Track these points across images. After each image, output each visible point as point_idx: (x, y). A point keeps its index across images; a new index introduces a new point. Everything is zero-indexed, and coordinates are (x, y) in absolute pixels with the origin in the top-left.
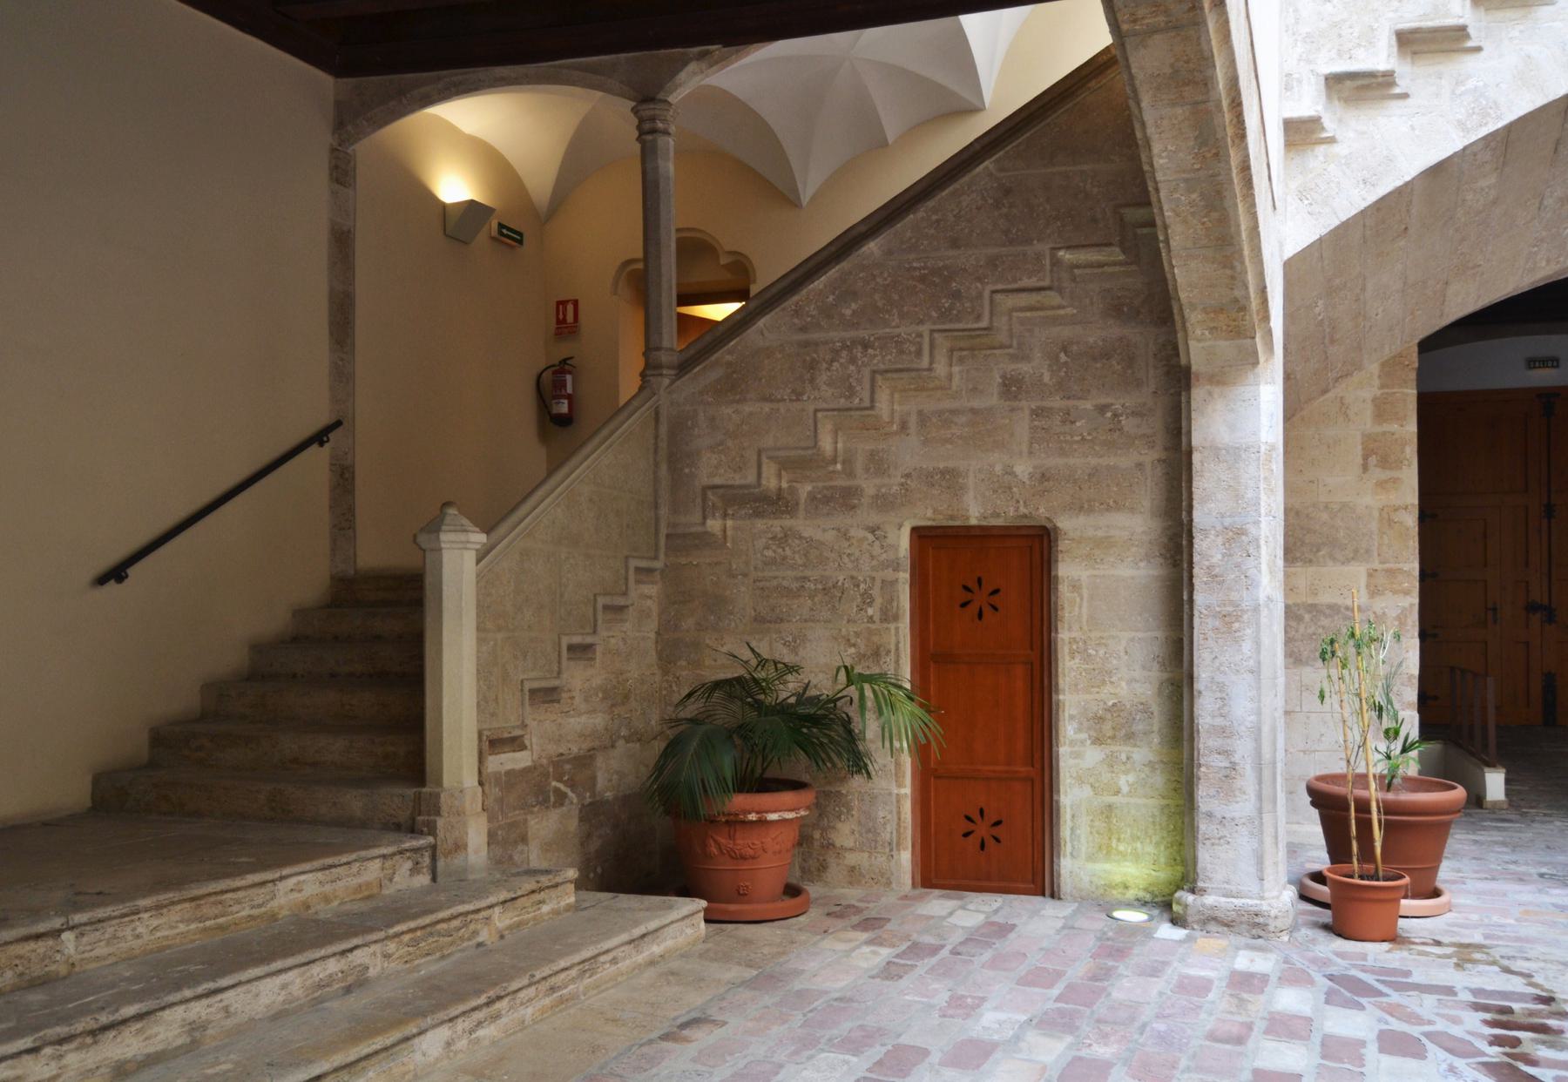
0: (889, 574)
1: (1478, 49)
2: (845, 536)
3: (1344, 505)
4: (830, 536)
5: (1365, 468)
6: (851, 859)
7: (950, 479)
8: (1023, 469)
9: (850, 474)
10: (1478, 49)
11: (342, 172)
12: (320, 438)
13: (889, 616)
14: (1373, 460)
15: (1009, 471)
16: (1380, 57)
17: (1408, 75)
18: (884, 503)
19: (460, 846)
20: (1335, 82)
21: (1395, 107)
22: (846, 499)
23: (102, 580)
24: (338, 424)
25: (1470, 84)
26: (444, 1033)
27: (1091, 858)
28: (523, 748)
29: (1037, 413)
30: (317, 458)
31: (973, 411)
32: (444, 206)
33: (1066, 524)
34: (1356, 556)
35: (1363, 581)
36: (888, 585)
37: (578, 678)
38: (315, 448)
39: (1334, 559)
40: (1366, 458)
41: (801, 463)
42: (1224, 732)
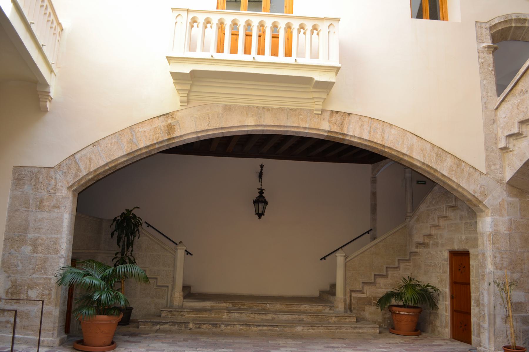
0: (444, 262)
4: (434, 253)
6: (439, 329)
8: (463, 238)
12: (368, 232)
15: (461, 238)
16: (516, 130)
18: (443, 246)
19: (337, 307)
22: (436, 244)
23: (321, 259)
24: (371, 230)
26: (302, 328)
31: (455, 224)
33: (471, 251)
38: (367, 234)
42: (483, 305)
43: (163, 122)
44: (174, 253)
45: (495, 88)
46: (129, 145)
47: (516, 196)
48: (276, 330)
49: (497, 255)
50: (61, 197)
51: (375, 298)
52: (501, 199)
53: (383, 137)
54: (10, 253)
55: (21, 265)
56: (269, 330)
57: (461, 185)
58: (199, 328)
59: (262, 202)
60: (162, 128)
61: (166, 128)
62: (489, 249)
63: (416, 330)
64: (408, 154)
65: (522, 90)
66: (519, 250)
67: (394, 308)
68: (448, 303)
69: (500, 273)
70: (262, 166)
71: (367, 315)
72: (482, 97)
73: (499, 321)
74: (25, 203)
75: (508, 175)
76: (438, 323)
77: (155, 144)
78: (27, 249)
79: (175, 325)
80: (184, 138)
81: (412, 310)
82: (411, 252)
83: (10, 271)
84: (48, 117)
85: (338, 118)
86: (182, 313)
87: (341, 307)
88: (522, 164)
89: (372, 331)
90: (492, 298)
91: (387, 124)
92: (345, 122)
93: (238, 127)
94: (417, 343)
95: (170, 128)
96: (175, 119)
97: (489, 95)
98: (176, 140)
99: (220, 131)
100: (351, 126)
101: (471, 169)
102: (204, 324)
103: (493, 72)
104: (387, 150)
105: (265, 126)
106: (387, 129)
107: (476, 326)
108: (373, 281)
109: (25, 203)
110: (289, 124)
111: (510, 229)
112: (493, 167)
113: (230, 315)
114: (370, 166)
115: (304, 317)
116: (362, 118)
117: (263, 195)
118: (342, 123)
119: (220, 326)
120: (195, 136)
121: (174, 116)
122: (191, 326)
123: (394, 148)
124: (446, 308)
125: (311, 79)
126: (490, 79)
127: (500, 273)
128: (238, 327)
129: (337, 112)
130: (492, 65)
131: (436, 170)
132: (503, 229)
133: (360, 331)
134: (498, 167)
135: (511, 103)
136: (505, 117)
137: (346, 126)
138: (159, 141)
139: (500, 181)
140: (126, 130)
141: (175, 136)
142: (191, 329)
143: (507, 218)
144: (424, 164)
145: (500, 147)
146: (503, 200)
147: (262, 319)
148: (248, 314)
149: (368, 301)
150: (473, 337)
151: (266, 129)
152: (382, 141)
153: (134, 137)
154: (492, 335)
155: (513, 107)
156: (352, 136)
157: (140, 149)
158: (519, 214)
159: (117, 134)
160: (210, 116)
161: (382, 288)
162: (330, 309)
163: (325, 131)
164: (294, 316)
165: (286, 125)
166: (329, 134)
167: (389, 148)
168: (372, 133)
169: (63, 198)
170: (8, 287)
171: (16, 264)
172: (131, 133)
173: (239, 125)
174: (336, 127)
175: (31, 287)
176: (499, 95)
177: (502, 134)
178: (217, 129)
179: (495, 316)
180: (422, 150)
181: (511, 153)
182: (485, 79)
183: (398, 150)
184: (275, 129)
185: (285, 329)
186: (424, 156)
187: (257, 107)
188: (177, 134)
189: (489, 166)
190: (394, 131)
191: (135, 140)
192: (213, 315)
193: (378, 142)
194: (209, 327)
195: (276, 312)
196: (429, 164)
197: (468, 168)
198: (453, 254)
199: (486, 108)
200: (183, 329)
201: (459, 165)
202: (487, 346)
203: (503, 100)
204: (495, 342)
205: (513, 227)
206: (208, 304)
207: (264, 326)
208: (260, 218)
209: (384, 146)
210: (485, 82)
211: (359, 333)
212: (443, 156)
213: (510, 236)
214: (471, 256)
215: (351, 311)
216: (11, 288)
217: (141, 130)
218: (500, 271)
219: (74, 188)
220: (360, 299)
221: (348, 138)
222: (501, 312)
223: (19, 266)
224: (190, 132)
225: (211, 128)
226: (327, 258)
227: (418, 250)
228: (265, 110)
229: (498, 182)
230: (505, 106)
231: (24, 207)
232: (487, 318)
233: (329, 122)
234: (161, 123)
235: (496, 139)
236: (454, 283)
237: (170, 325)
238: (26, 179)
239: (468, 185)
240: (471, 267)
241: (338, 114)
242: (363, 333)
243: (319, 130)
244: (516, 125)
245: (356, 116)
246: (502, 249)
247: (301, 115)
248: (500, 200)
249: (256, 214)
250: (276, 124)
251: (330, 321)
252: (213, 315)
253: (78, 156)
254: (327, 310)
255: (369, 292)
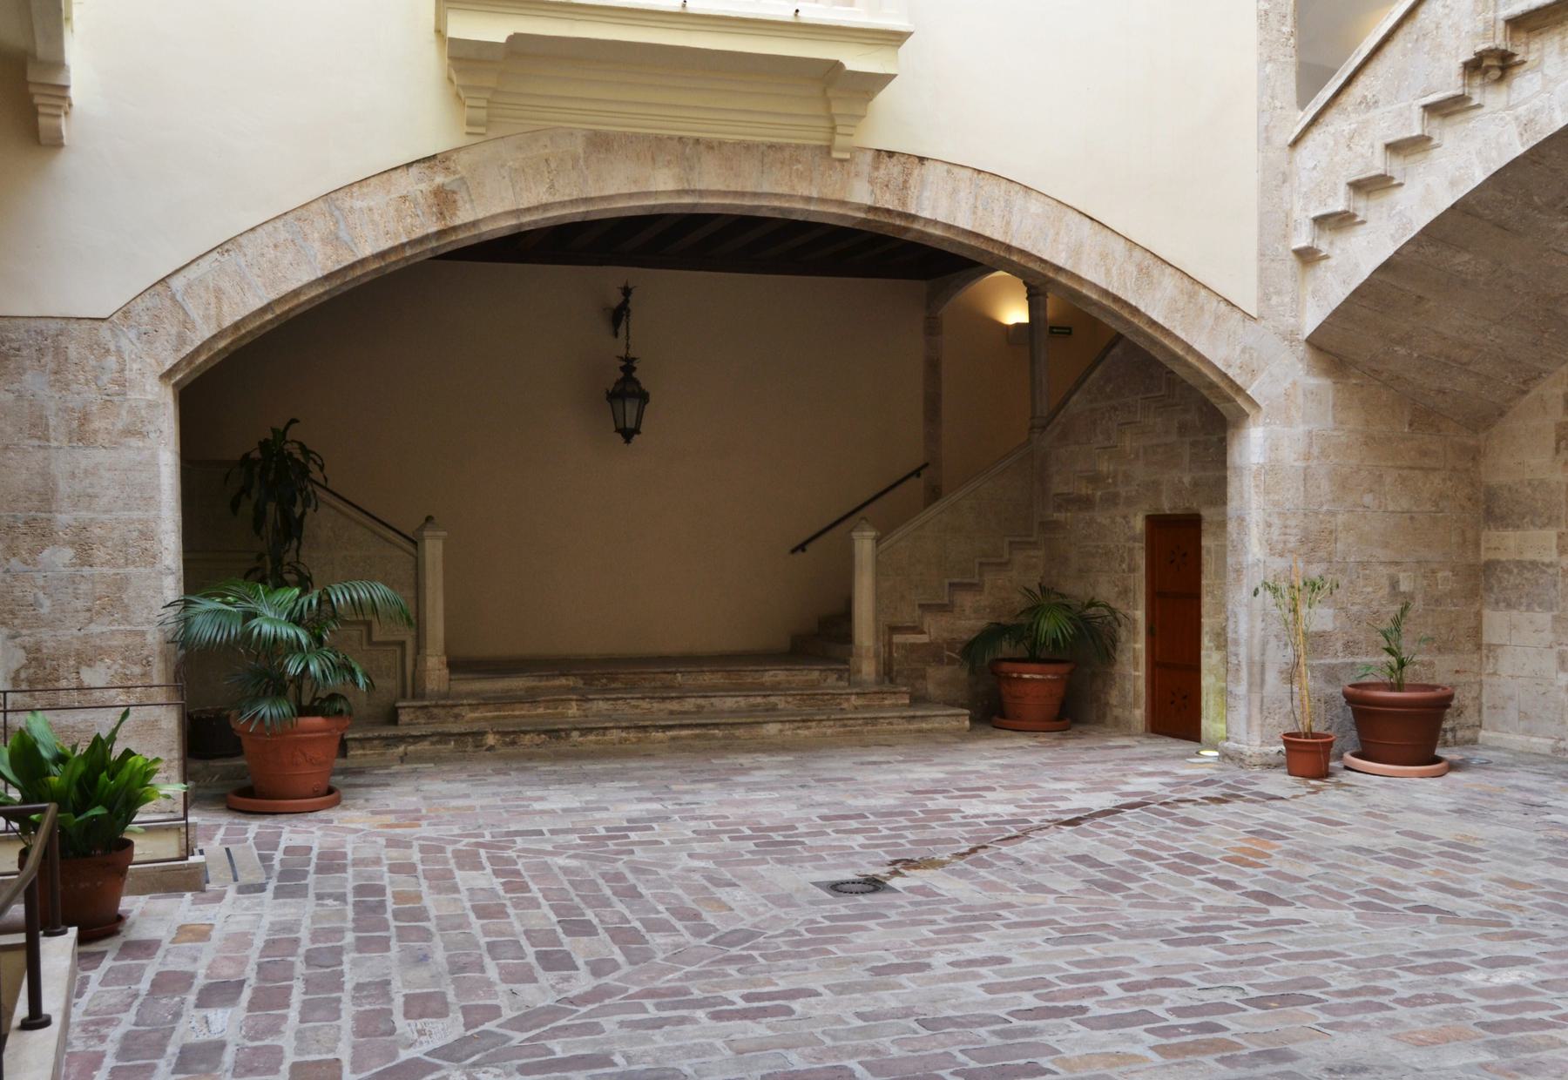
0: (1130, 544)
1: (1401, 185)
2: (1113, 522)
3: (1542, 482)
5: (1557, 451)
6: (1117, 712)
7: (1155, 487)
8: (1187, 479)
9: (1115, 484)
10: (1401, 185)
11: (932, 327)
12: (917, 473)
13: (1132, 570)
14: (1563, 444)
15: (1181, 481)
16: (1338, 204)
17: (1362, 206)
18: (1130, 502)
19: (859, 671)
20: (1321, 221)
21: (1360, 230)
22: (1112, 500)
23: (794, 551)
24: (926, 465)
25: (1398, 208)
26: (779, 726)
27: (1214, 720)
28: (922, 632)
29: (1194, 444)
30: (916, 484)
32: (1007, 327)
33: (1207, 513)
34: (1550, 521)
35: (1555, 541)
36: (1131, 550)
37: (966, 600)
38: (914, 478)
39: (1533, 523)
40: (1558, 444)
41: (1095, 479)
42: (1236, 642)
43: (421, 180)
44: (412, 550)
45: (1293, 86)
46: (329, 250)
47: (1327, 373)
48: (714, 737)
49: (1276, 521)
50: (143, 404)
51: (951, 644)
52: (1290, 380)
53: (1008, 223)
54: (8, 571)
55: (47, 603)
56: (697, 736)
57: (1196, 346)
58: (513, 743)
59: (633, 395)
60: (421, 201)
61: (431, 200)
62: (1254, 506)
63: (1059, 718)
64: (1068, 267)
65: (1365, 97)
66: (1325, 508)
67: (1006, 667)
68: (1141, 645)
69: (1279, 564)
70: (627, 292)
71: (931, 688)
72: (1261, 112)
73: (1272, 678)
74: (34, 426)
75: (1311, 320)
76: (1114, 697)
77: (403, 245)
78: (60, 557)
79: (447, 743)
80: (484, 228)
81: (1052, 667)
82: (1042, 524)
83: (16, 622)
84: (67, 163)
85: (893, 169)
86: (456, 710)
87: (868, 669)
88: (1348, 292)
89: (954, 723)
90: (1259, 625)
91: (1017, 188)
92: (912, 182)
93: (631, 196)
94: (1071, 744)
95: (443, 199)
96: (455, 173)
97: (1278, 104)
98: (461, 235)
99: (582, 209)
100: (926, 194)
101: (1223, 305)
102: (525, 732)
103: (1292, 41)
104: (1015, 258)
105: (701, 193)
106: (1018, 199)
107: (1212, 697)
108: (946, 601)
109: (34, 426)
110: (766, 188)
111: (1307, 457)
112: (1275, 300)
113: (588, 705)
114: (922, 286)
115: (779, 701)
116: (956, 170)
117: (635, 375)
118: (905, 186)
119: (568, 736)
120: (514, 222)
121: (452, 165)
122: (491, 740)
123: (1034, 252)
124: (1135, 658)
125: (837, 65)
126: (1282, 59)
127: (1279, 564)
128: (615, 735)
129: (891, 154)
130: (1290, 20)
131: (1135, 310)
132: (1290, 456)
133: (924, 725)
134: (1287, 299)
135: (1331, 129)
136: (1315, 167)
137: (913, 191)
138: (414, 236)
139: (1289, 337)
140: (314, 205)
141: (458, 222)
142: (491, 748)
143: (1300, 429)
144: (1106, 293)
145: (1295, 247)
146: (1294, 384)
147: (672, 713)
148: (633, 702)
149: (934, 654)
150: (1204, 722)
151: (704, 201)
152: (1006, 233)
153: (342, 225)
154: (1255, 711)
155: (1336, 143)
156: (928, 221)
157: (363, 262)
158: (1330, 418)
159: (289, 218)
160: (553, 165)
161: (968, 620)
162: (840, 678)
163: (859, 207)
164: (751, 700)
165: (759, 190)
166: (871, 217)
167: (1022, 252)
168: (980, 213)
169: (151, 406)
170: (15, 665)
171: (30, 599)
172: (332, 215)
173: (634, 189)
174: (887, 196)
175: (85, 659)
176: (1302, 104)
177: (1304, 211)
178: (573, 202)
179: (1263, 666)
180: (1104, 256)
181: (1323, 263)
182: (1270, 59)
183: (1045, 257)
184: (727, 201)
185: (737, 733)
186: (1108, 272)
187: (680, 138)
188: (464, 216)
189: (1265, 298)
190: (1035, 206)
191: (342, 234)
192: (541, 711)
193: (996, 236)
194: (537, 740)
195: (706, 692)
196: (1120, 294)
197: (1215, 304)
198: (1156, 523)
199: (1268, 140)
200: (470, 749)
201: (1192, 296)
202: (1244, 738)
203: (1314, 121)
204: (1262, 725)
205: (1315, 451)
206: (517, 683)
207: (682, 726)
208: (628, 441)
209: (1009, 248)
210: (1269, 68)
211: (920, 731)
212: (1155, 273)
213: (1307, 476)
214: (1204, 526)
215: (892, 681)
216: (24, 667)
217: (358, 204)
218: (1278, 560)
219: (179, 377)
220: (914, 647)
221: (917, 226)
222: (1278, 657)
223: (41, 606)
224: (499, 210)
225: (558, 198)
226: (808, 548)
227: (1059, 516)
228: (702, 148)
229: (1285, 339)
230: (1316, 135)
231: (32, 437)
232: (1244, 674)
233: (871, 181)
234: (415, 185)
235: (1288, 227)
236: (1157, 597)
237: (433, 743)
238: (25, 353)
239: (1214, 345)
240: (1204, 552)
241: (894, 160)
242: (930, 731)
243: (843, 203)
244: (1343, 190)
245: (939, 165)
246: (1288, 505)
247: (799, 162)
248: (1287, 385)
249: (618, 430)
250: (733, 188)
251: (845, 705)
252: (541, 711)
253: (177, 283)
254: (832, 679)
255: (935, 629)
